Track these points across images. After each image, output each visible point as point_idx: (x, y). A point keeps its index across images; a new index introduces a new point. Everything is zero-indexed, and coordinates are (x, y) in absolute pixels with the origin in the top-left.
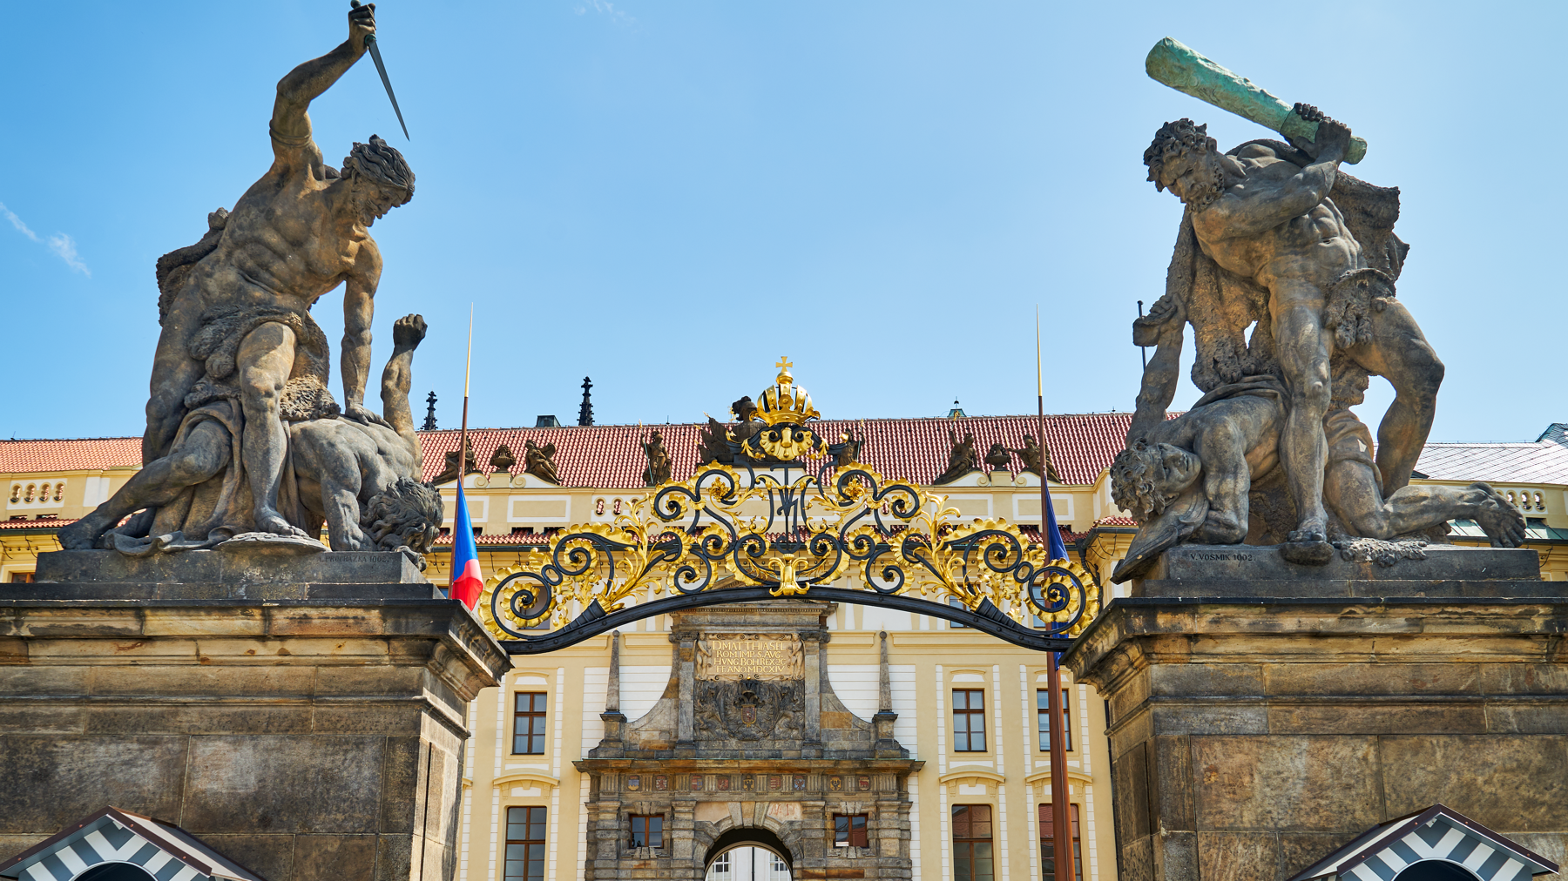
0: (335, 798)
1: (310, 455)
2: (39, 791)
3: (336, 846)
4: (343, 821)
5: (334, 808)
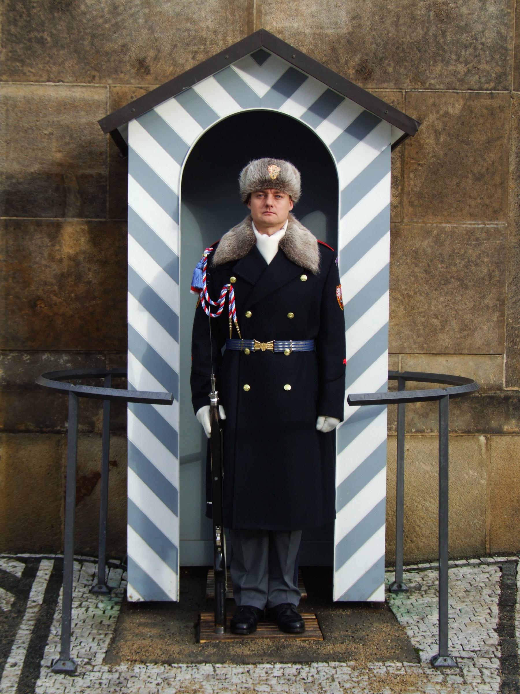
0: (453, 42)
2: (62, 26)
3: (459, 105)
4: (466, 74)
5: (453, 57)
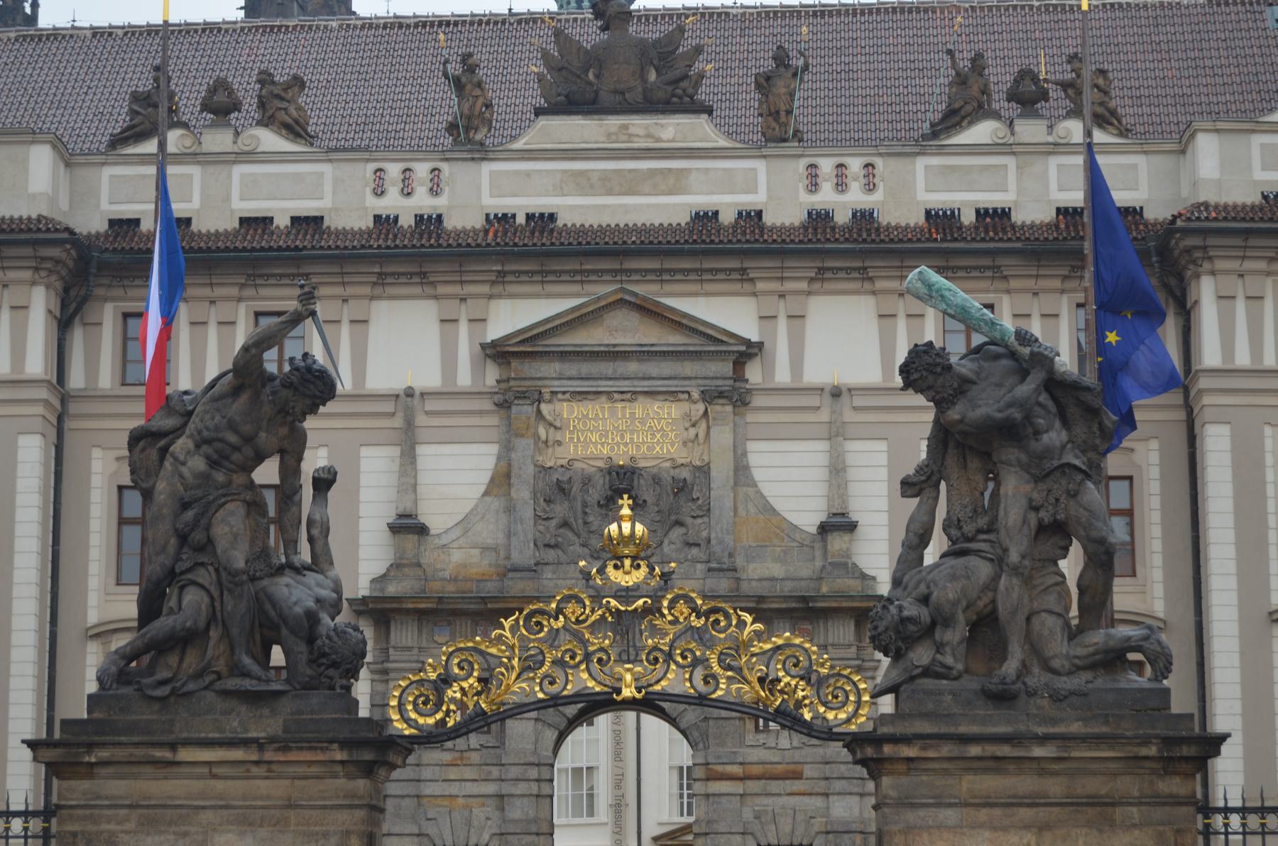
1: (272, 613)
